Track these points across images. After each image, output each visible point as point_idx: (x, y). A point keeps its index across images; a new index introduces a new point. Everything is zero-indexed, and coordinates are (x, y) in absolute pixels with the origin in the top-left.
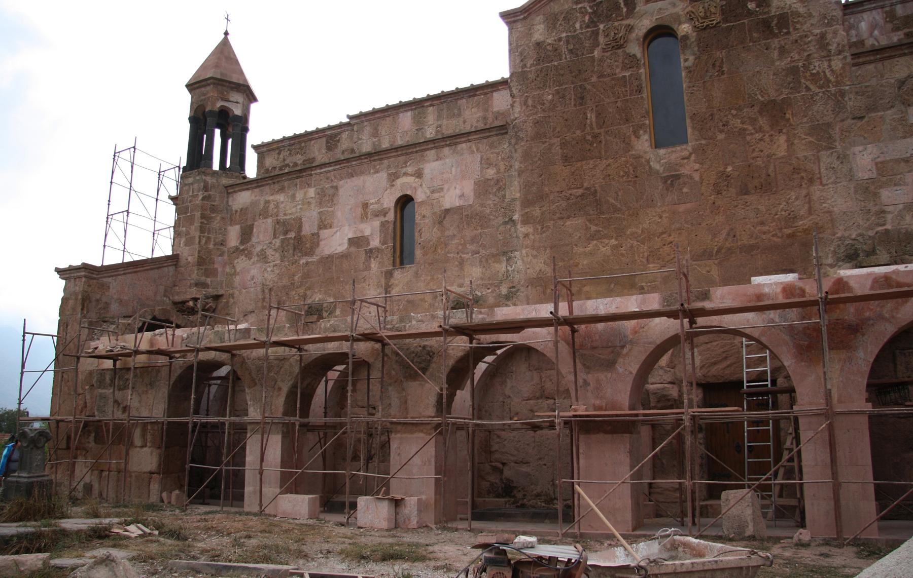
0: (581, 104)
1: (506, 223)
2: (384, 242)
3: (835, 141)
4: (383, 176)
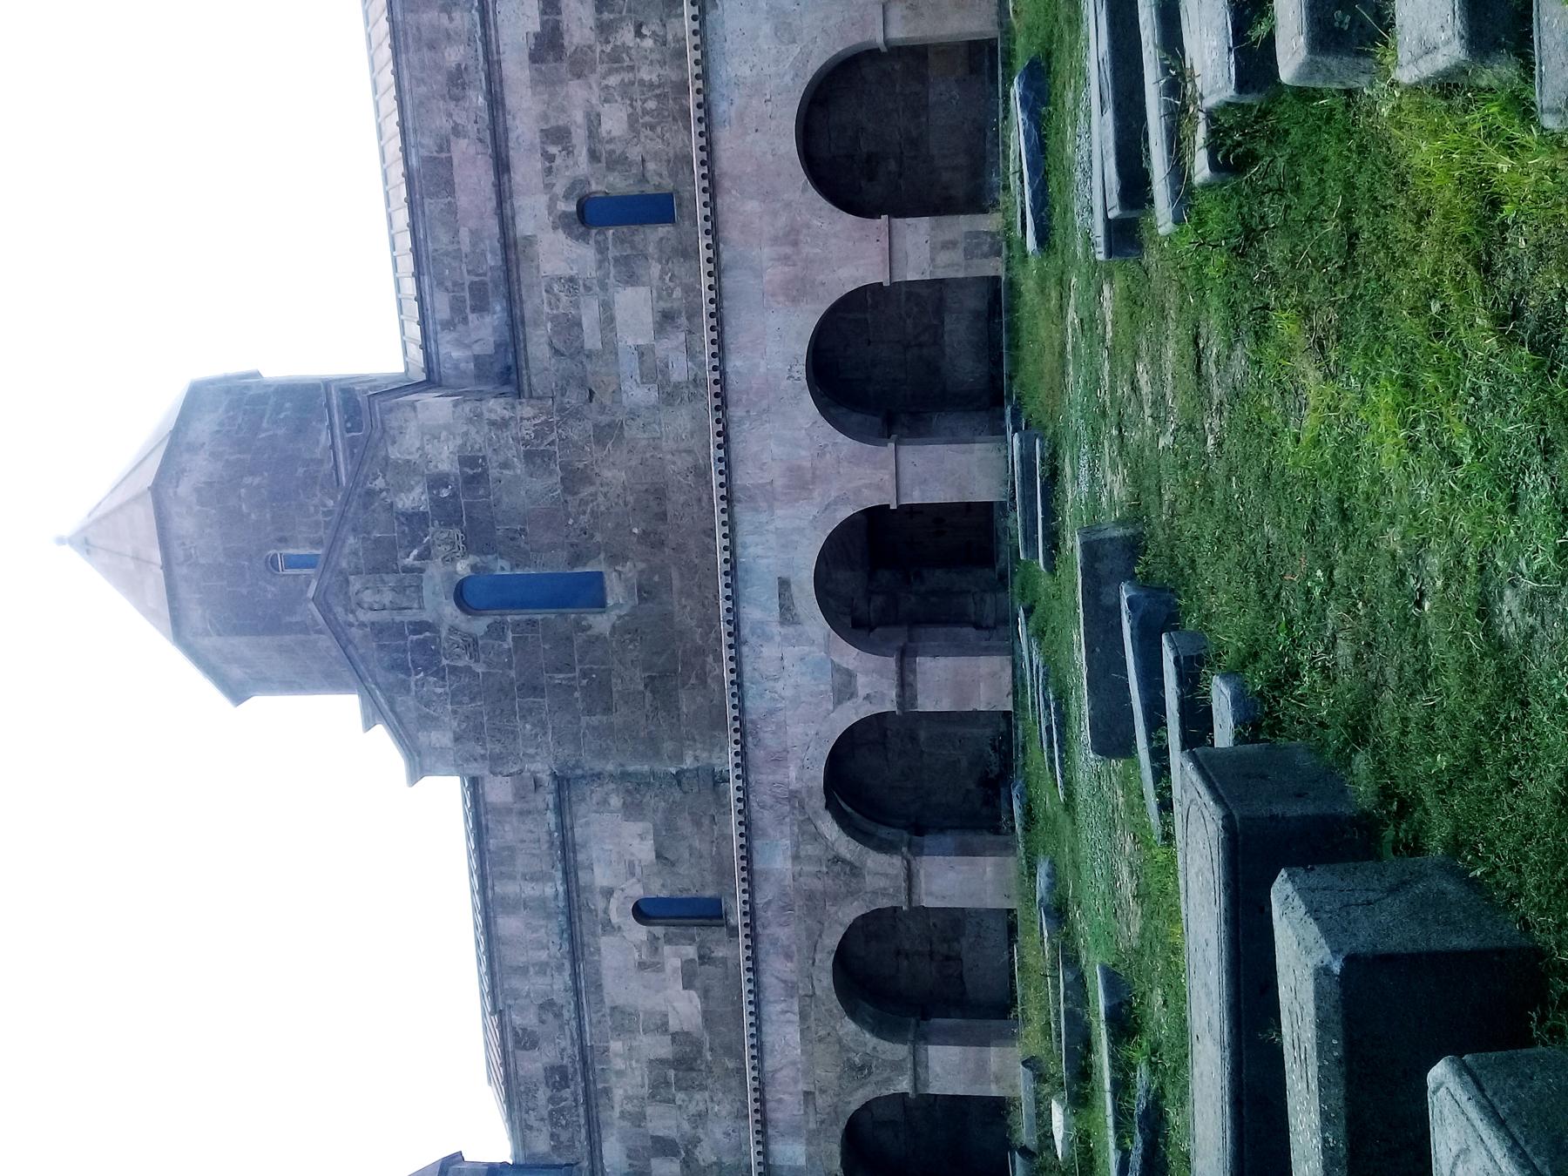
1: (679, 783)
2: (692, 940)
3: (614, 421)
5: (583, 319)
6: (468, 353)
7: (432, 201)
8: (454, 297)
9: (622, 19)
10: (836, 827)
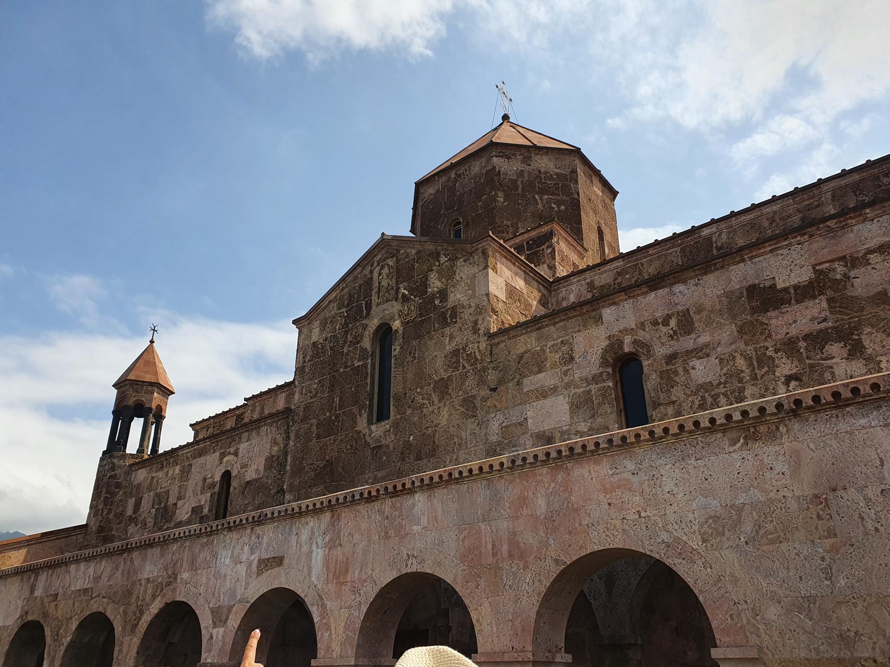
1: (278, 492)
2: (210, 511)
3: (477, 410)
5: (544, 373)
9: (801, 361)
10: (156, 611)
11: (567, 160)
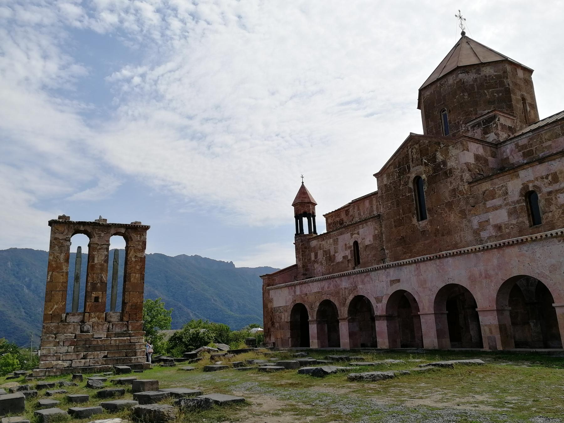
0: (398, 207)
1: (382, 249)
2: (352, 257)
4: (349, 234)
6: (509, 155)
7: (559, 128)
8: (527, 145)
10: (351, 299)
11: (501, 67)
